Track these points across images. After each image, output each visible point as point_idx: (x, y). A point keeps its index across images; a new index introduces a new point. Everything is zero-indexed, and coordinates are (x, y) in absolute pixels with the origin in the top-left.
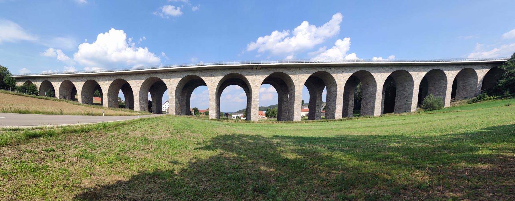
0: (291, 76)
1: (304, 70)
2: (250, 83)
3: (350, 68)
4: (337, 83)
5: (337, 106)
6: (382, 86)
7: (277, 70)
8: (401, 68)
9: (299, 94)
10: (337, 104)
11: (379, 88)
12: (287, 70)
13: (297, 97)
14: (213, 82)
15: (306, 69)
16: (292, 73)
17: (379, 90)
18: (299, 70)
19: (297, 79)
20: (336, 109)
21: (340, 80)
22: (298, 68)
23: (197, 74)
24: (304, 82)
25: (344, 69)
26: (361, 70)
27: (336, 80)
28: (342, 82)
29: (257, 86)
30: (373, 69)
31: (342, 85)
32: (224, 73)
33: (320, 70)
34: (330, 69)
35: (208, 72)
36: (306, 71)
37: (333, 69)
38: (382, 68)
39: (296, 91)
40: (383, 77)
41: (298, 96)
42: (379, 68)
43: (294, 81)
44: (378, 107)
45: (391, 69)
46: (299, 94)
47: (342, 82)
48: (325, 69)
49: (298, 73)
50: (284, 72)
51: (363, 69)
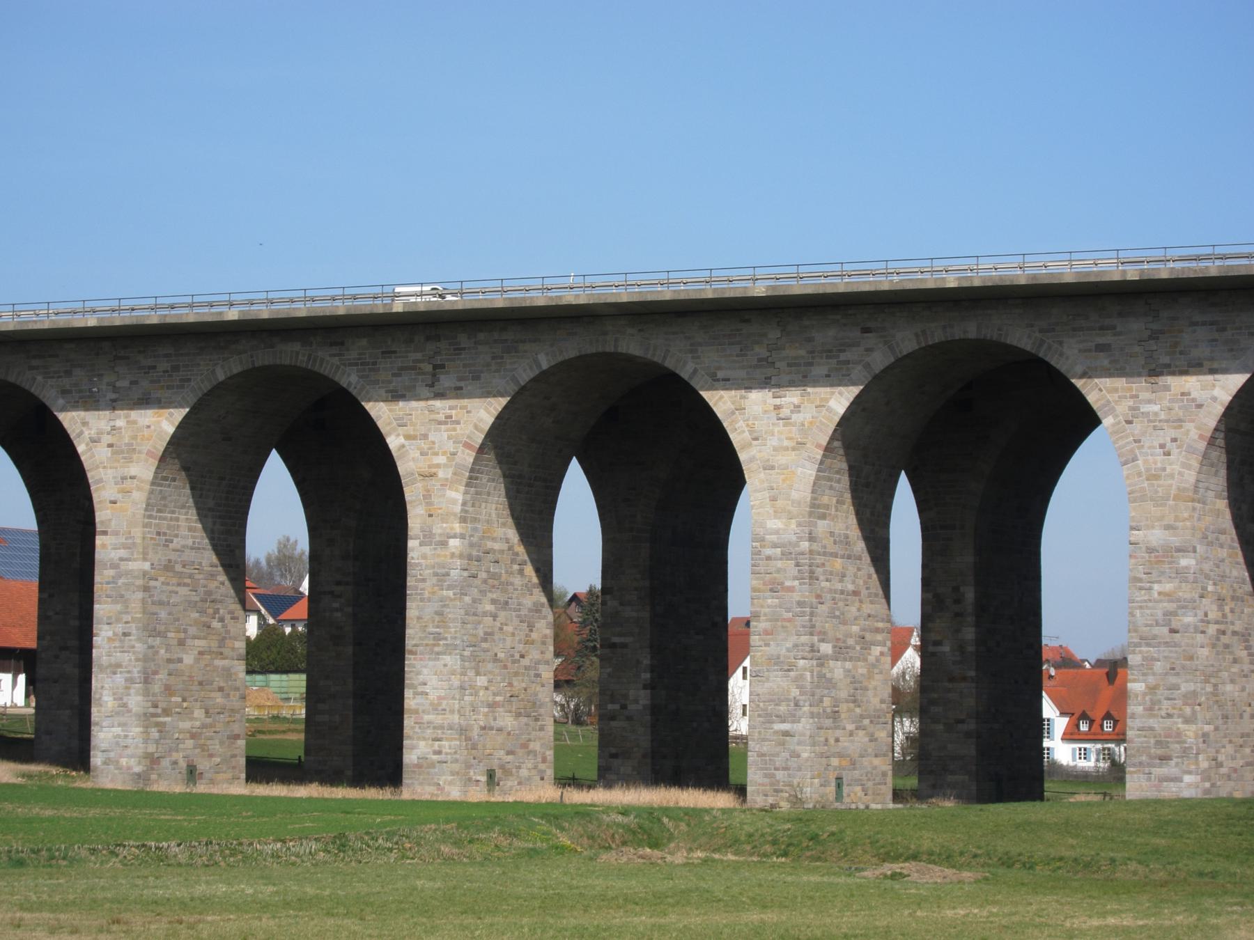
1: (148, 362)
4: (404, 467)
5: (410, 661)
6: (795, 495)
8: (969, 329)
9: (122, 553)
10: (409, 643)
11: (777, 514)
12: (35, 362)
13: (110, 573)
16: (66, 382)
17: (774, 538)
19: (100, 433)
20: (408, 693)
21: (425, 436)
24: (149, 453)
26: (590, 349)
27: (393, 442)
28: (441, 460)
33: (264, 357)
34: (335, 350)
36: (164, 365)
38: (774, 334)
39: (99, 528)
40: (797, 408)
41: (114, 566)
43: (80, 449)
44: (783, 708)
45: (866, 330)
46: (125, 547)
47: (441, 460)
48: (297, 346)
49: (106, 379)
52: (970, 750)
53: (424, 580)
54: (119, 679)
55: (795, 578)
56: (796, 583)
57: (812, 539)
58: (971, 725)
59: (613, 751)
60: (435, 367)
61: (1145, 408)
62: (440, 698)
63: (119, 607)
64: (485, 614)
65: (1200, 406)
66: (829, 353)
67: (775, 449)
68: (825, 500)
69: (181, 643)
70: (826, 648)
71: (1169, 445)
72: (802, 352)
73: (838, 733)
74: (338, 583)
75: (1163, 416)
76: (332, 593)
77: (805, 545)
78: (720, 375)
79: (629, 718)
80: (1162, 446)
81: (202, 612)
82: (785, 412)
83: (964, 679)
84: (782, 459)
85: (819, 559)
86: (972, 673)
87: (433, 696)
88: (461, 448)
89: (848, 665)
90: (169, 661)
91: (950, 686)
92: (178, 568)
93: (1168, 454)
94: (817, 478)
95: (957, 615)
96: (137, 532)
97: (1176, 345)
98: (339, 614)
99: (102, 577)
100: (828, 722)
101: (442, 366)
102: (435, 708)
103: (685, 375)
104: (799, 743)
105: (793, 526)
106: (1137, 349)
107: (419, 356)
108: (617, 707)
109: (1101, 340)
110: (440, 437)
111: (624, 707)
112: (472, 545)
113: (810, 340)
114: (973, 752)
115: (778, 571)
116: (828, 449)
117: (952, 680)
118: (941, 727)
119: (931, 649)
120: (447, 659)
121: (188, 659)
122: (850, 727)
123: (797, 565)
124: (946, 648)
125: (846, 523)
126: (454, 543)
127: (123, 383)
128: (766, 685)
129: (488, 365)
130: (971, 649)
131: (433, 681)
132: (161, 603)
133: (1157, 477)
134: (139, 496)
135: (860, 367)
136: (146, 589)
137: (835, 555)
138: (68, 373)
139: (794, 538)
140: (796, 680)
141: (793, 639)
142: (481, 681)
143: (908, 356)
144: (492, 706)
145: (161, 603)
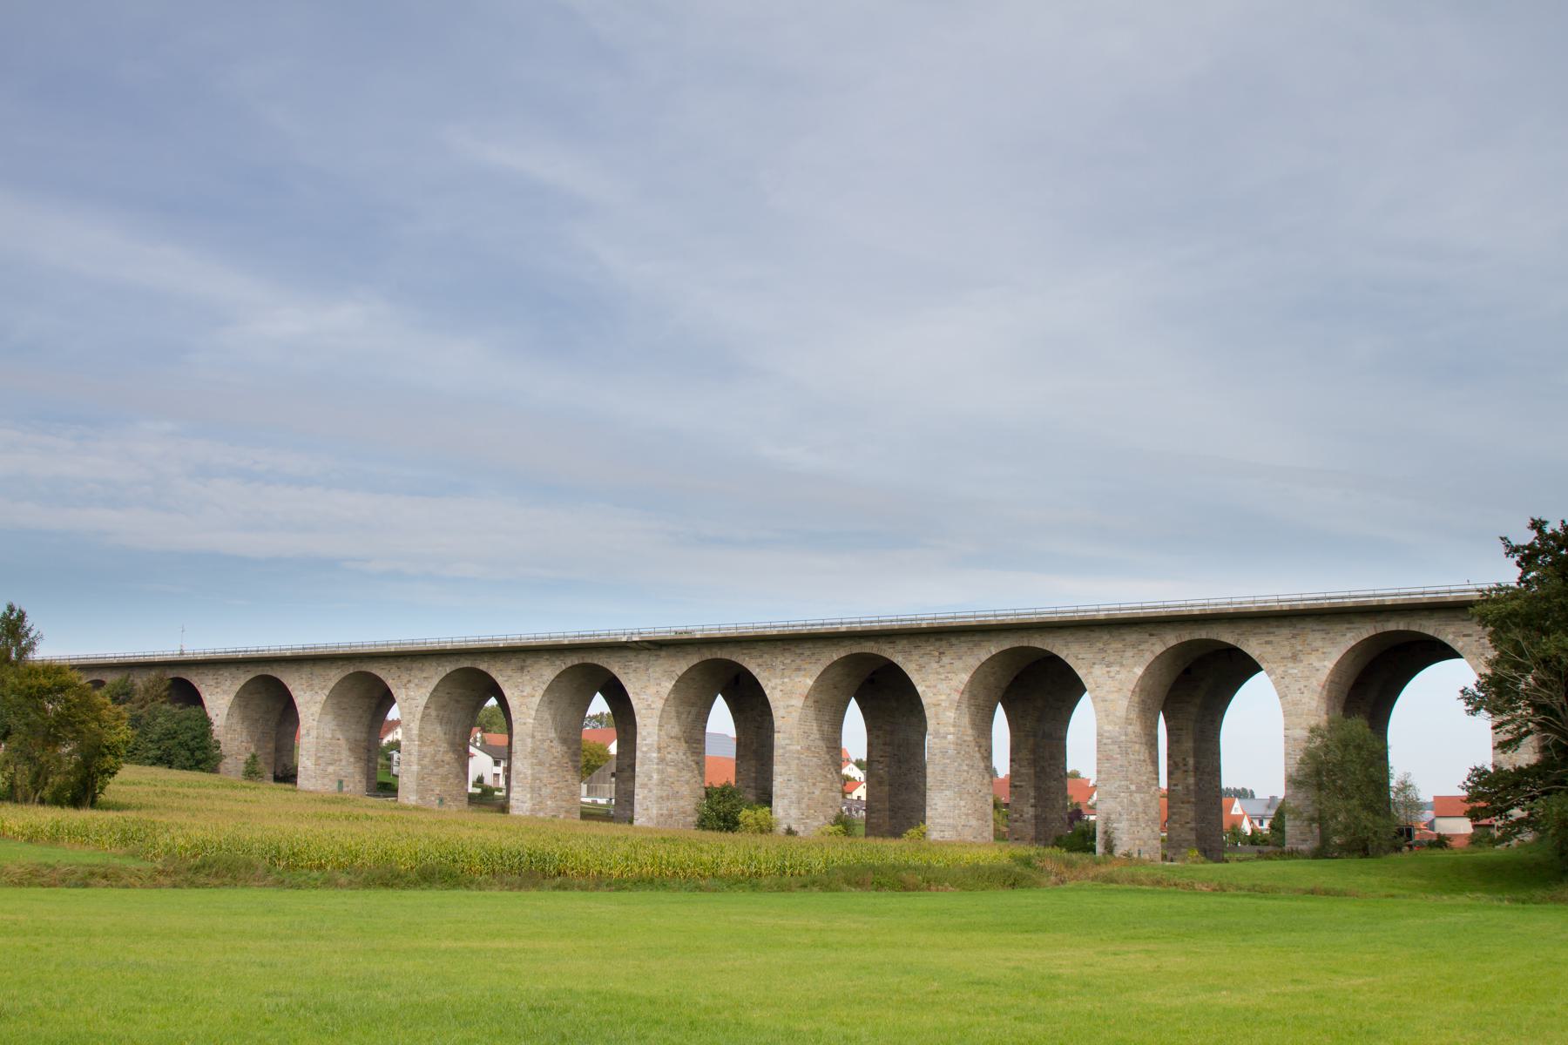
0: (759, 674)
1: (801, 651)
2: (631, 696)
3: (969, 639)
5: (928, 793)
7: (714, 650)
8: (1202, 634)
9: (787, 742)
10: (928, 785)
13: (781, 751)
14: (525, 694)
15: (807, 646)
16: (760, 661)
17: (1107, 734)
18: (784, 649)
20: (928, 809)
21: (935, 686)
22: (779, 643)
23: (483, 667)
25: (944, 643)
26: (1016, 645)
27: (920, 689)
28: (943, 697)
29: (652, 707)
30: (1070, 638)
31: (945, 709)
32: (558, 663)
34: (891, 645)
35: (514, 661)
36: (808, 653)
37: (902, 644)
38: (1106, 637)
39: (776, 730)
41: (783, 748)
42: (1093, 635)
43: (767, 692)
45: (1151, 635)
47: (943, 697)
48: (872, 644)
49: (779, 659)
50: (733, 659)
51: (1025, 639)
52: (1193, 837)
53: (935, 755)
54: (786, 801)
55: (1118, 754)
56: (1118, 756)
57: (1126, 735)
58: (1193, 825)
59: (1016, 837)
60: (940, 653)
61: (1290, 671)
62: (944, 811)
63: (785, 767)
64: (964, 771)
65: (1318, 670)
66: (1133, 646)
67: (1107, 692)
68: (1131, 716)
69: (814, 784)
70: (1133, 787)
71: (1303, 688)
72: (1120, 646)
73: (1139, 828)
74: (881, 757)
75: (1299, 675)
76: (878, 761)
77: (1123, 738)
78: (1080, 656)
79: (1024, 821)
80: (1300, 689)
81: (823, 770)
82: (1112, 674)
83: (1189, 802)
84: (1111, 697)
85: (1130, 745)
86: (1193, 800)
87: (940, 810)
88: (953, 692)
89: (1142, 795)
90: (809, 793)
91: (1182, 805)
92: (813, 749)
93: (1303, 693)
94: (1129, 705)
95: (1186, 771)
96: (795, 732)
97: (1305, 641)
98: (881, 771)
99: (777, 752)
100: (1134, 823)
101: (944, 653)
102: (941, 816)
103: (1062, 657)
104: (1122, 833)
105: (1117, 728)
106: (1286, 643)
107: (932, 648)
108: (1018, 816)
109: (1267, 639)
110: (943, 686)
111: (1021, 816)
112: (958, 738)
113: (1124, 640)
114: (1194, 838)
115: (1110, 750)
116: (1133, 692)
117: (1183, 803)
118: (1178, 825)
119: (1173, 788)
120: (947, 792)
121: (817, 792)
122: (1143, 825)
123: (1119, 747)
124: (1180, 788)
125: (1136, 728)
126: (950, 737)
127: (789, 661)
128: (1105, 805)
129: (966, 652)
130: (1192, 788)
131: (940, 803)
132: (805, 765)
133: (1297, 704)
134: (796, 715)
135: (1148, 653)
136: (799, 759)
137: (1136, 742)
138: (761, 656)
139: (1117, 734)
140: (1119, 803)
141: (1118, 783)
142: (962, 803)
143: (1172, 647)
144: (967, 815)
145: (805, 765)
